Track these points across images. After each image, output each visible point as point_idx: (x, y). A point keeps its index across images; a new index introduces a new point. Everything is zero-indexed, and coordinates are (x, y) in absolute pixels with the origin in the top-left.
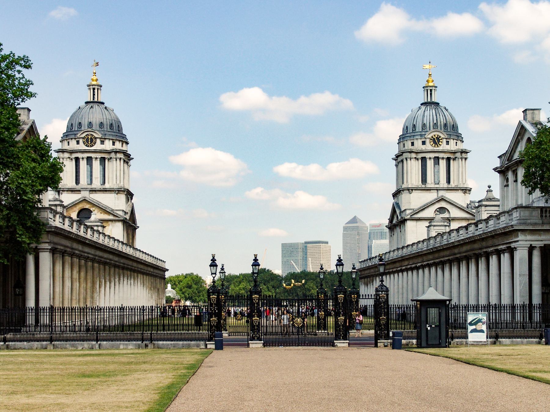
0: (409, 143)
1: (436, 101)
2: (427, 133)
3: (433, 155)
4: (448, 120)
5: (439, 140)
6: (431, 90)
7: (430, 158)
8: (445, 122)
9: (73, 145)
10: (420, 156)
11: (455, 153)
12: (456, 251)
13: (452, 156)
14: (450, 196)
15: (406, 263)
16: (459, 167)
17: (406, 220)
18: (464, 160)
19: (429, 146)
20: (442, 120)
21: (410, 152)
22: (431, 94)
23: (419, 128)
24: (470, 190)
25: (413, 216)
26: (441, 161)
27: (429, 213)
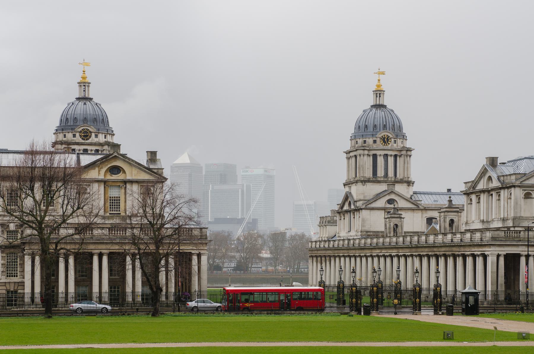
1: (385, 104)
3: (383, 153)
5: (388, 139)
6: (380, 94)
7: (380, 155)
8: (393, 124)
9: (70, 136)
15: (378, 251)
16: (405, 163)
17: (362, 209)
18: (408, 157)
19: (379, 144)
22: (380, 97)
23: (371, 128)
24: (413, 183)
25: (368, 206)
26: (389, 158)
27: (381, 203)
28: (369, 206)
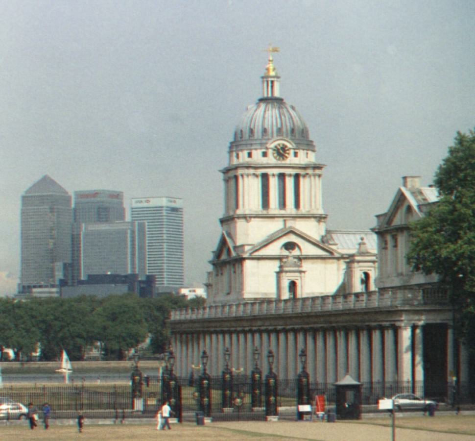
0: (246, 153)
2: (270, 142)
3: (277, 171)
4: (296, 124)
7: (273, 175)
8: (292, 126)
10: (260, 172)
11: (305, 168)
12: (333, 319)
13: (302, 172)
14: (301, 226)
15: (259, 323)
17: (244, 259)
19: (271, 159)
20: (288, 124)
21: (248, 167)
27: (275, 249)
28: (257, 254)
